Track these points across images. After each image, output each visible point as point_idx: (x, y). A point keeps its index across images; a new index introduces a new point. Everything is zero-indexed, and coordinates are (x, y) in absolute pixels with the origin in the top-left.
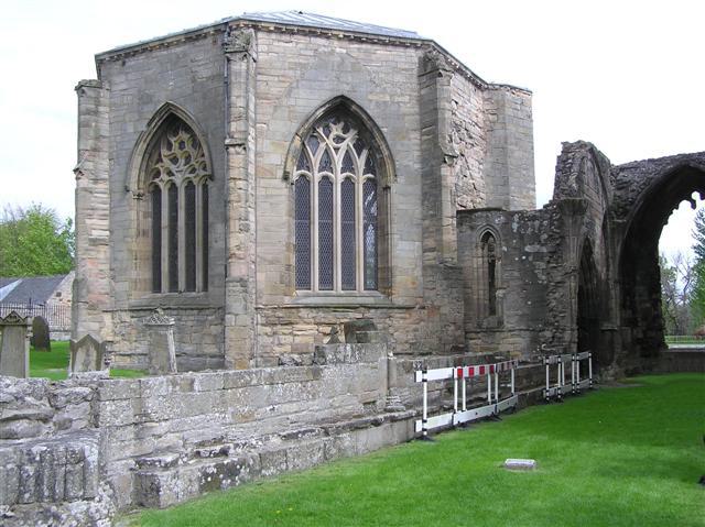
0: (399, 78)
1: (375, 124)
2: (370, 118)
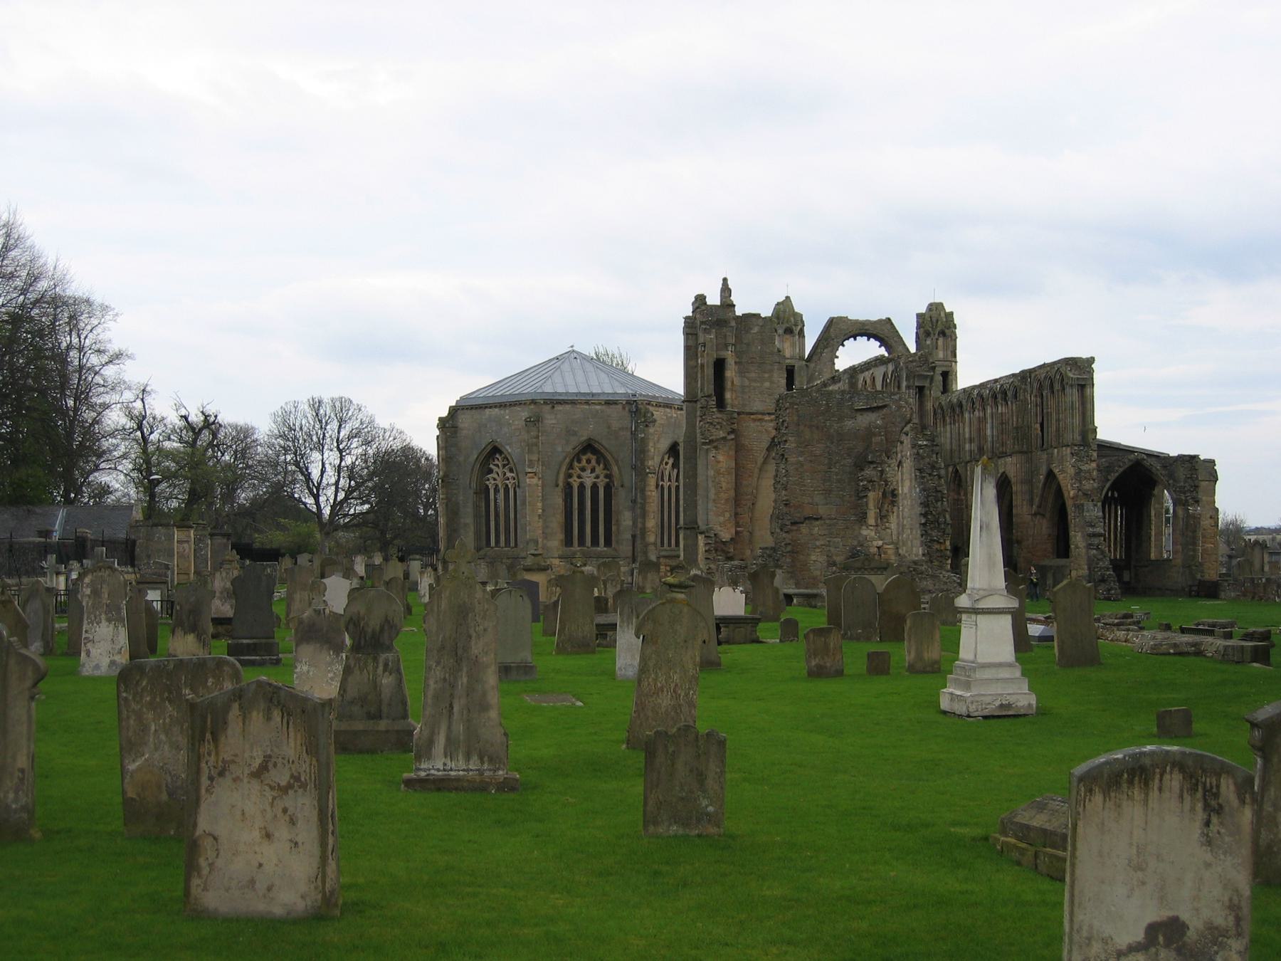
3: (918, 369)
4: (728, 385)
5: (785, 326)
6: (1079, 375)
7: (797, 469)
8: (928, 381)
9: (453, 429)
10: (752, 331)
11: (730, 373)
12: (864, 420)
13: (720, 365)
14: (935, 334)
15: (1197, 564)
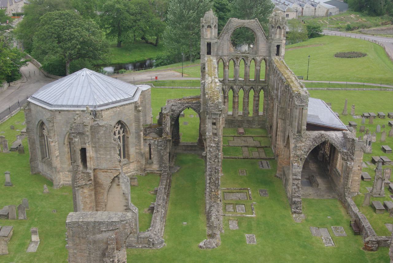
0: (130, 112)
1: (126, 124)
2: (125, 123)
3: (213, 110)
4: (88, 159)
5: (208, 24)
6: (301, 103)
7: (74, 255)
8: (219, 116)
9: (29, 110)
10: (100, 133)
11: (90, 153)
12: (105, 235)
13: (83, 151)
14: (275, 28)
15: (348, 188)
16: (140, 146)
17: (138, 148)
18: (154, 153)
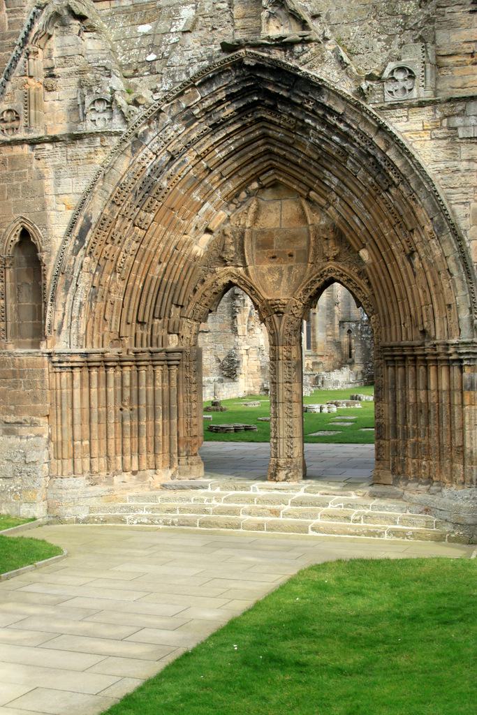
16: (333, 329)
17: (330, 333)
18: (356, 345)
